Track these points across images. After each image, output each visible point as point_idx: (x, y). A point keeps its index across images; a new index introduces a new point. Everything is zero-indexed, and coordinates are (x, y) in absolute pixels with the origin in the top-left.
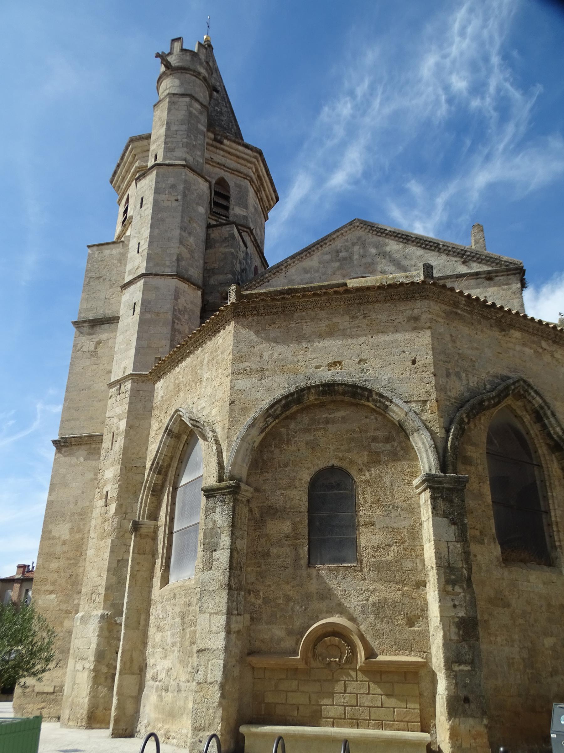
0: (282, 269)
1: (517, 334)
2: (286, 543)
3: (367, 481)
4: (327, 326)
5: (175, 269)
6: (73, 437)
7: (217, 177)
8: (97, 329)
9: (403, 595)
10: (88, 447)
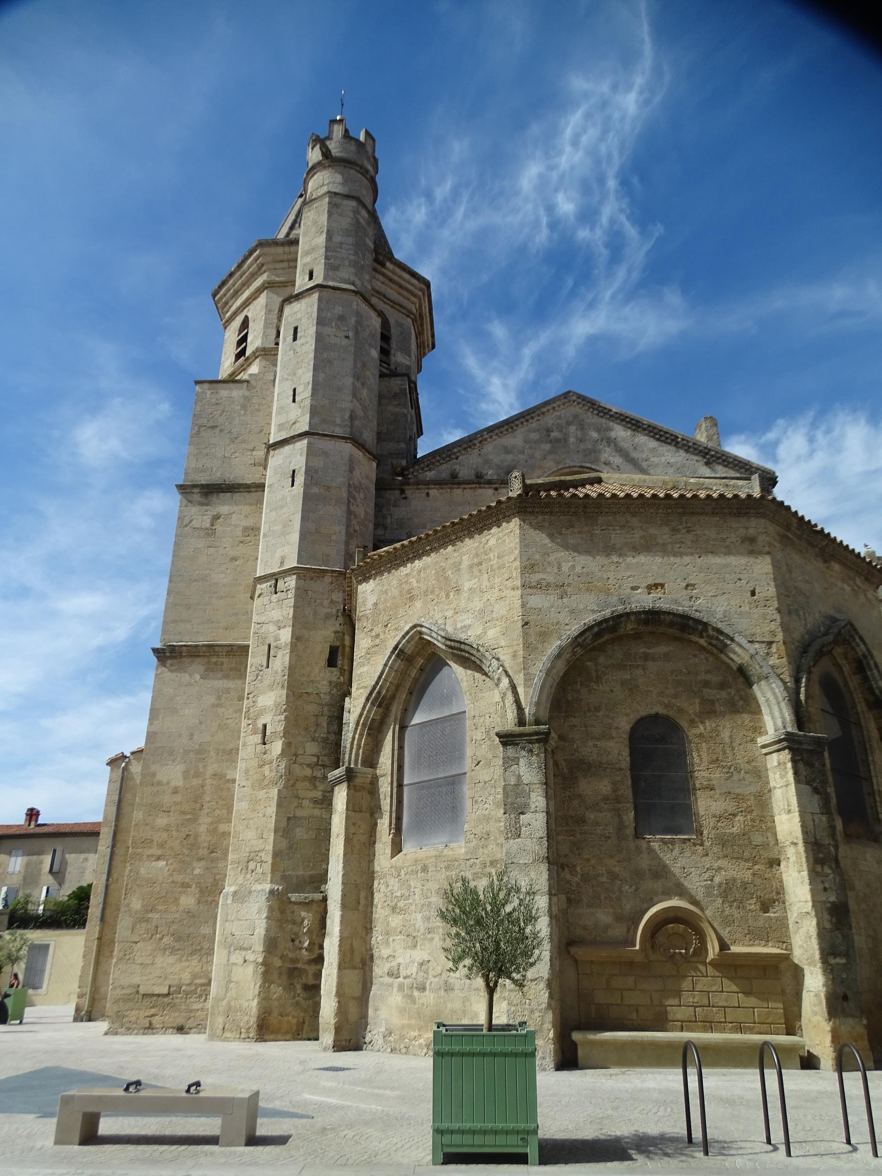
0: (475, 445)
1: (837, 567)
3: (701, 736)
4: (642, 538)
5: (348, 430)
6: (185, 646)
8: (214, 498)
9: (754, 875)
10: (206, 660)
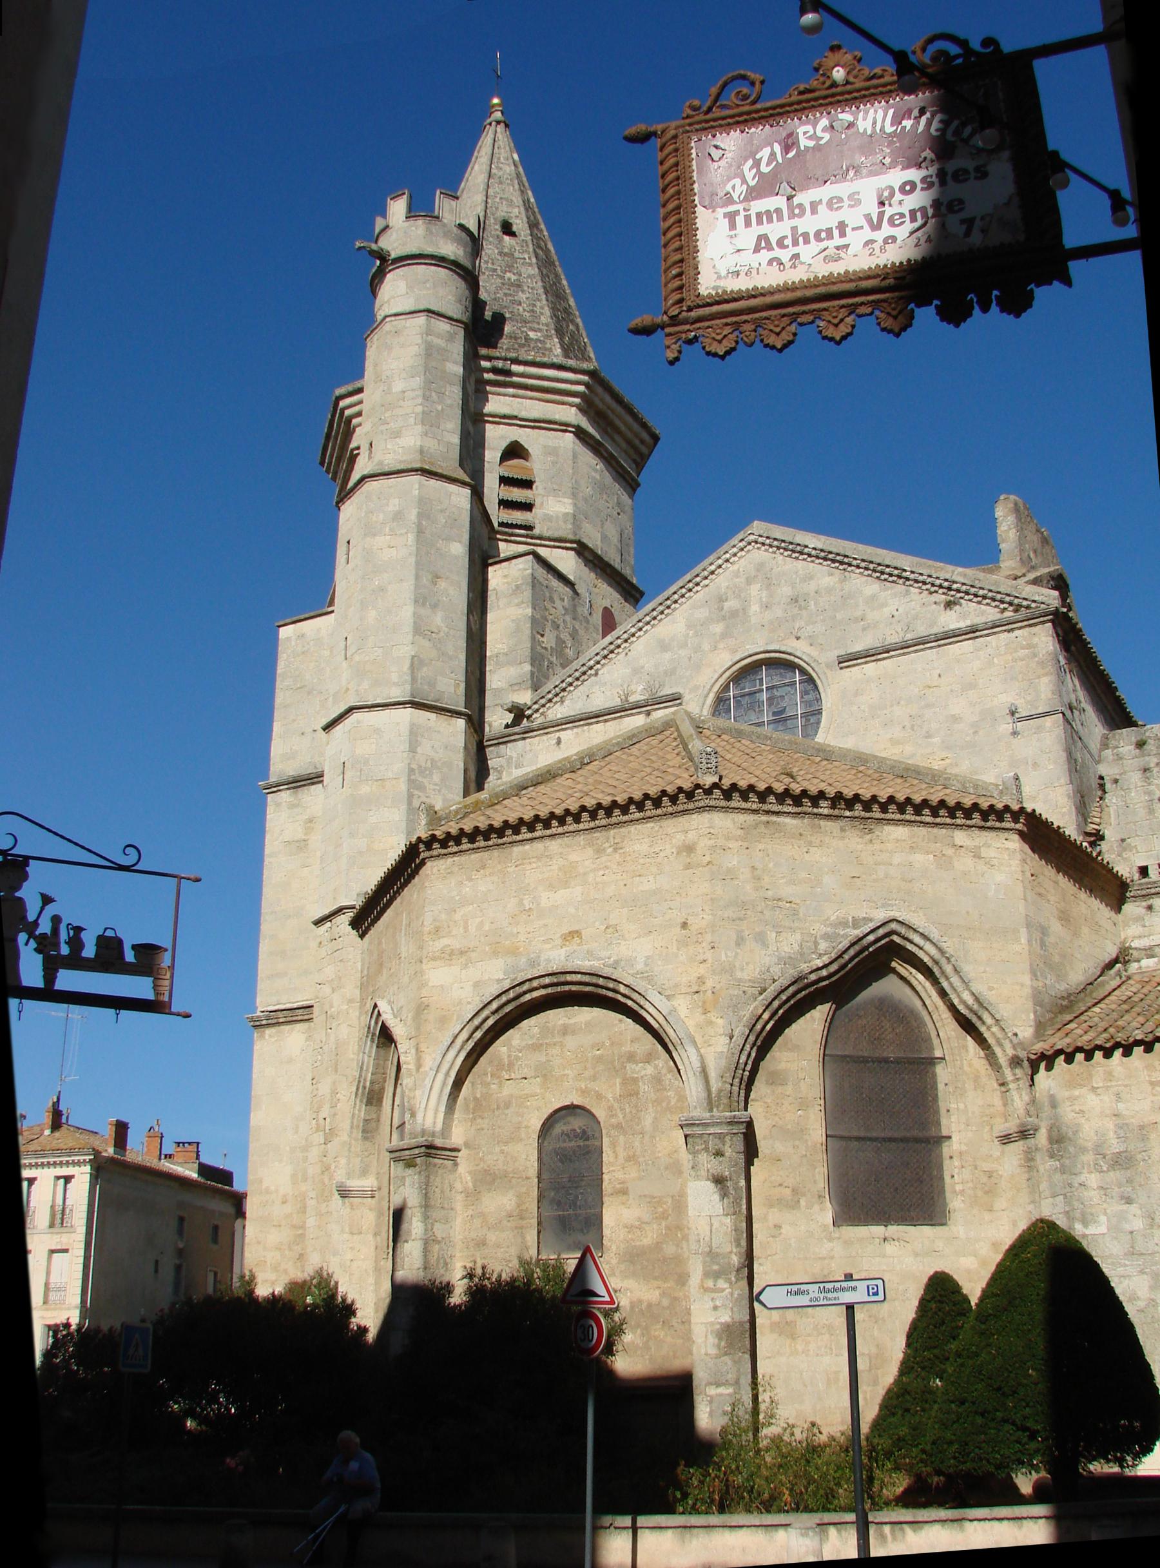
2: (509, 1224)
4: (560, 869)
5: (408, 687)
7: (504, 444)
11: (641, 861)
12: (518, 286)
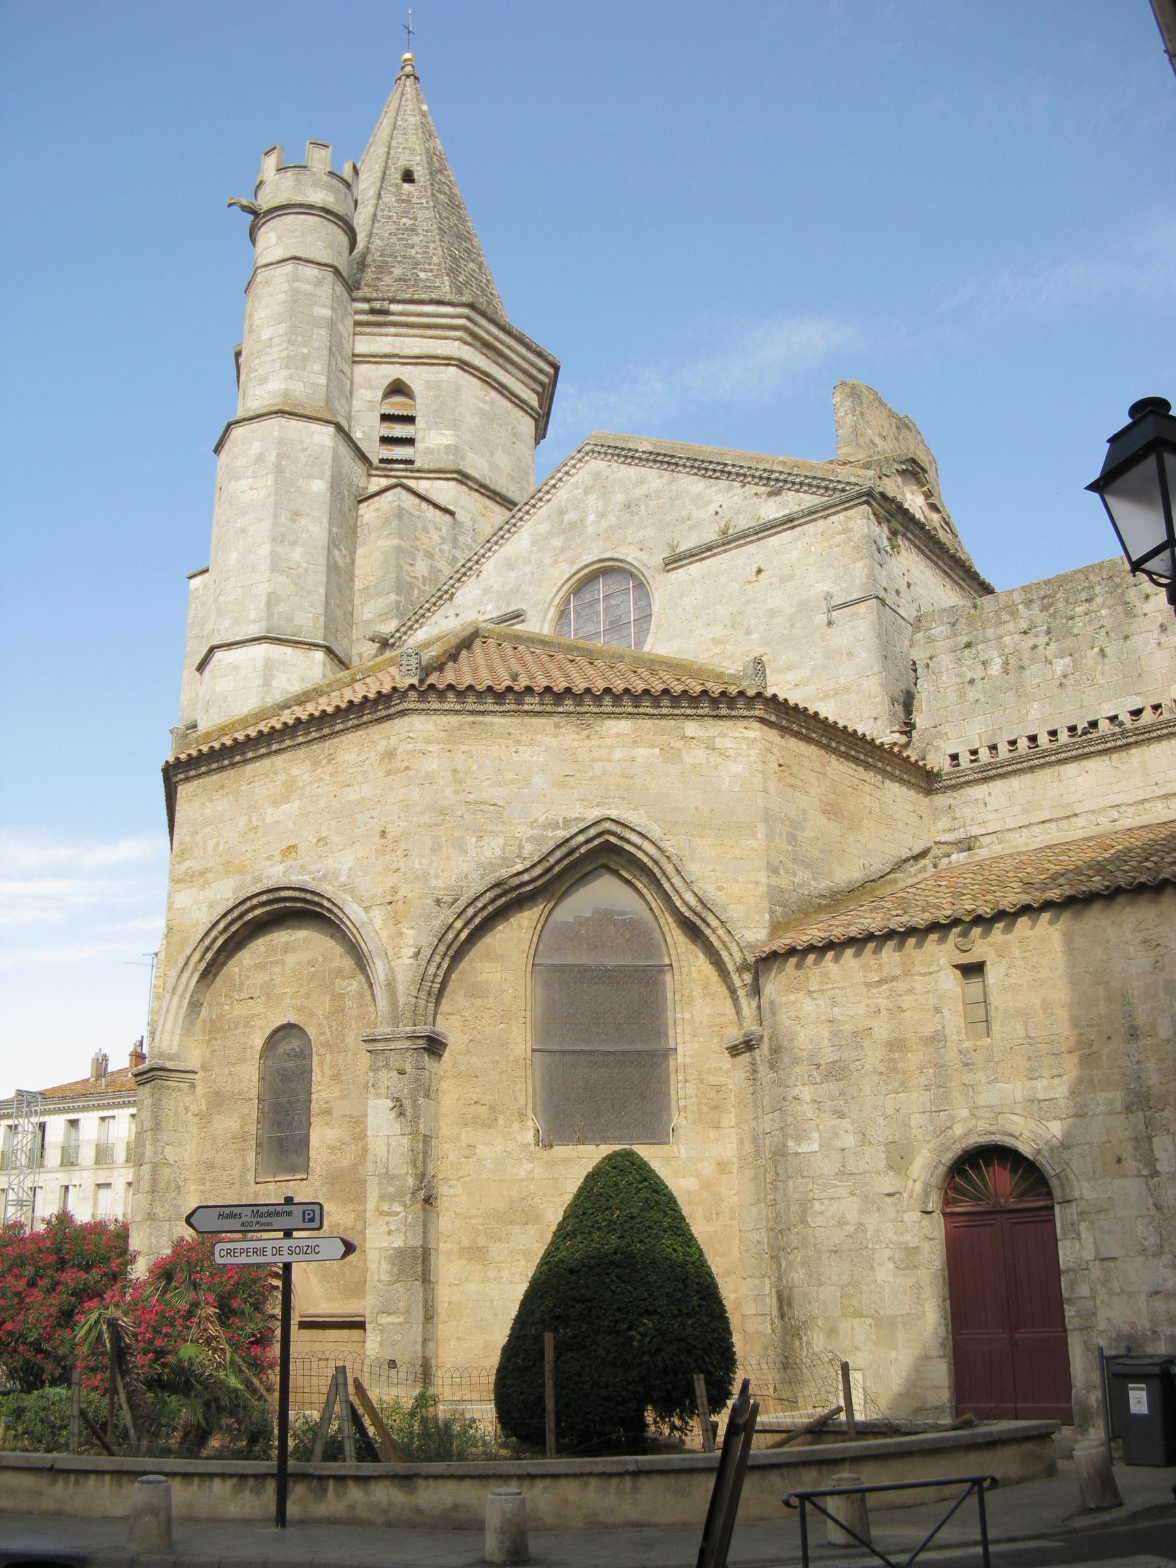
5: (264, 624)
7: (386, 382)
11: (350, 771)
12: (413, 230)
